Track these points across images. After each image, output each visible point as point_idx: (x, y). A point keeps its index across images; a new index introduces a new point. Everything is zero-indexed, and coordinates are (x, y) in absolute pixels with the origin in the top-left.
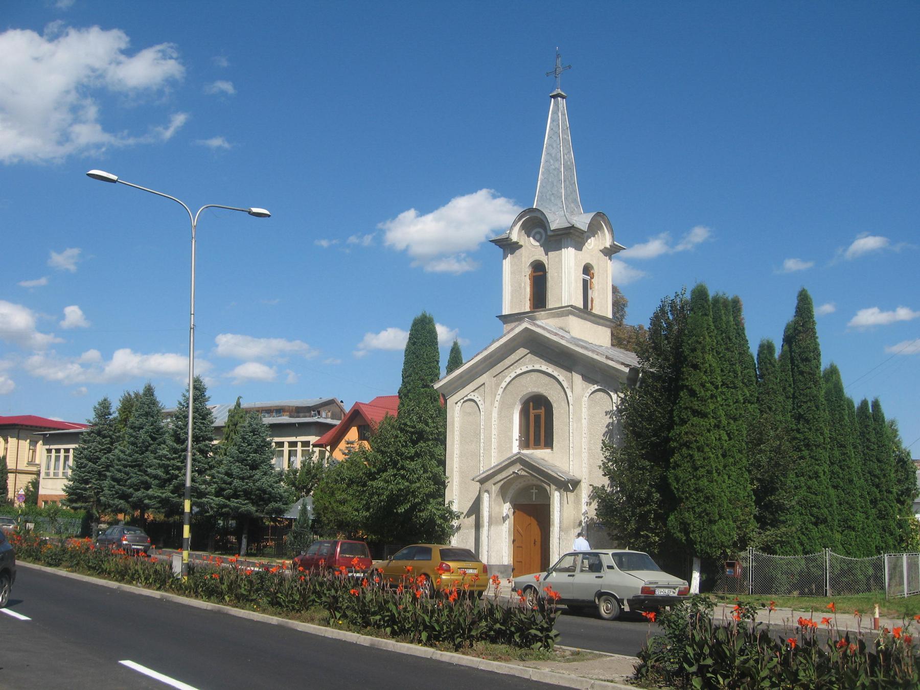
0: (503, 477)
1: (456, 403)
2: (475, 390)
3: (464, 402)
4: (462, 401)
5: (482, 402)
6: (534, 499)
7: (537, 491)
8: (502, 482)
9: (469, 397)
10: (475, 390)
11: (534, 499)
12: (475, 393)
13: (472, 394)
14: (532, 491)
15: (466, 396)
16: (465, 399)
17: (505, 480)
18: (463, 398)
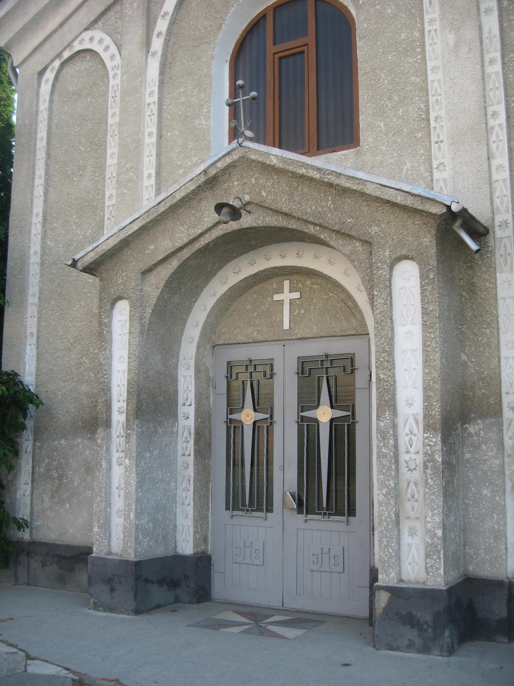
0: (179, 244)
1: (42, 73)
2: (95, 21)
3: (63, 65)
4: (57, 64)
5: (113, 49)
6: (286, 326)
7: (297, 295)
8: (175, 263)
9: (77, 47)
10: (95, 21)
11: (286, 326)
12: (97, 34)
13: (87, 35)
14: (277, 297)
15: (69, 45)
16: (66, 55)
17: (186, 253)
18: (59, 55)
